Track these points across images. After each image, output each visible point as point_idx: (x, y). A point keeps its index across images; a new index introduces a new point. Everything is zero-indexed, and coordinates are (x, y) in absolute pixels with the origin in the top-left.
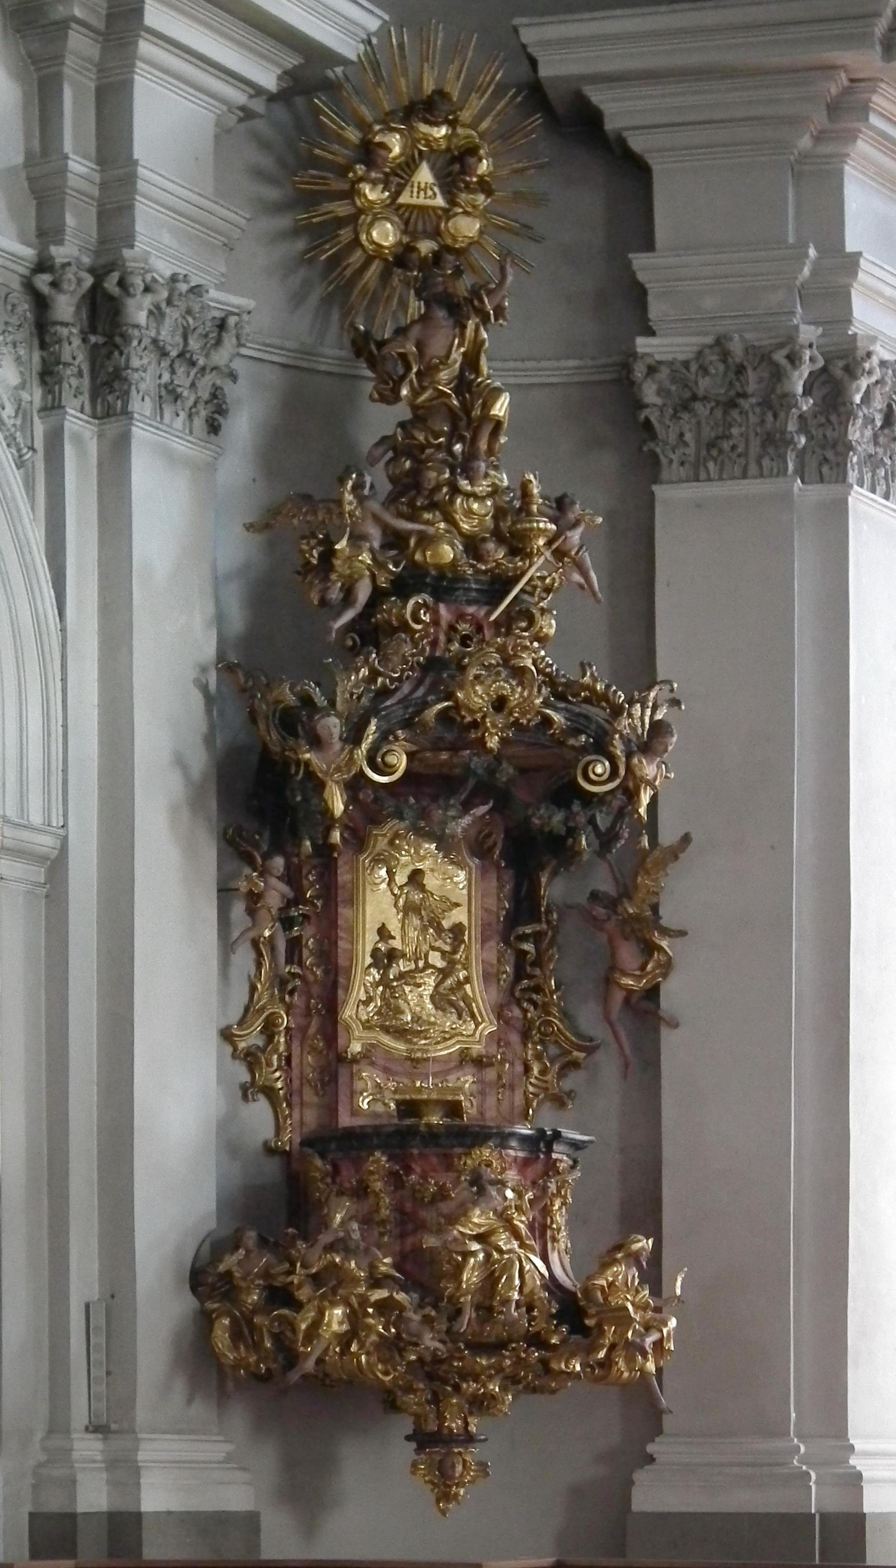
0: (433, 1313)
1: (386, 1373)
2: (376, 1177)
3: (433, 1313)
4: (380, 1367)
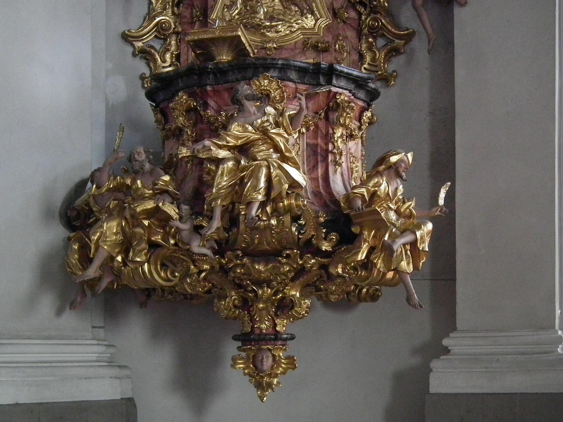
2: (177, 112)
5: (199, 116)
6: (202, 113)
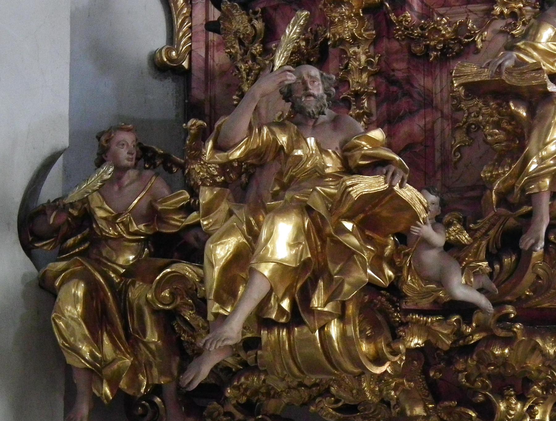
0: (465, 237)
1: (378, 360)
3: (465, 237)
4: (364, 347)
5: (384, 23)
6: (393, 17)
